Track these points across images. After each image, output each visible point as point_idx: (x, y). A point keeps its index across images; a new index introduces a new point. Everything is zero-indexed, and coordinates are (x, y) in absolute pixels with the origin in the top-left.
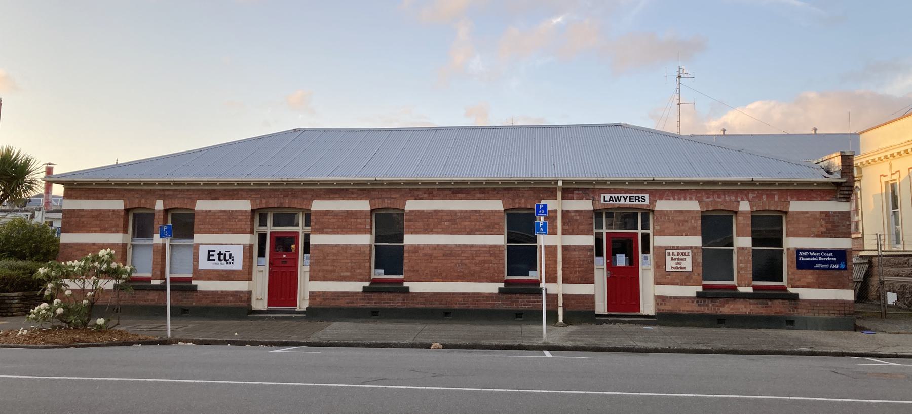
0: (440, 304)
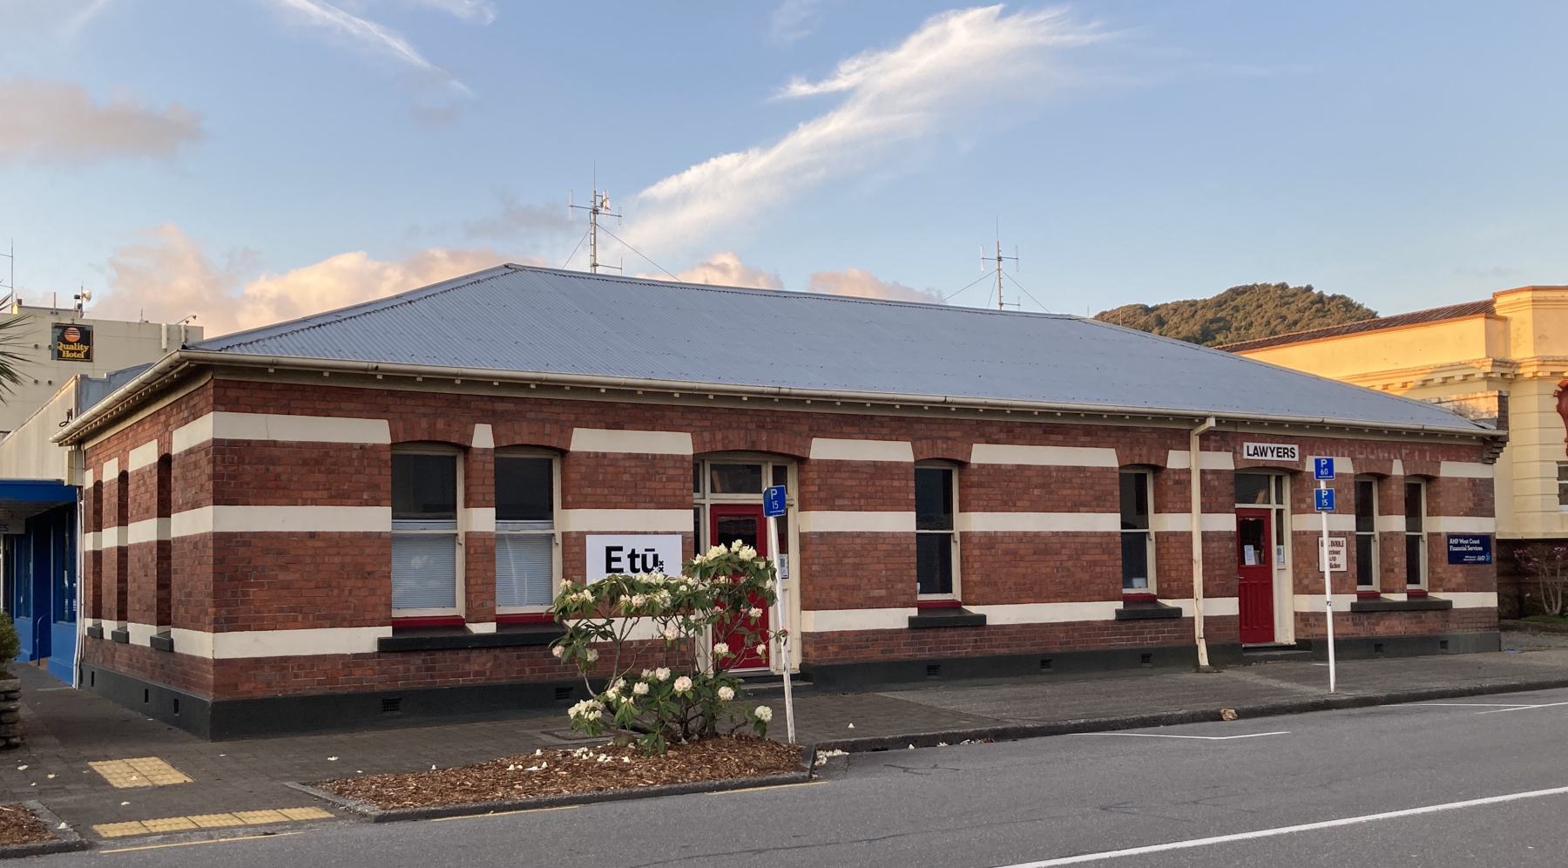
0: (1033, 645)
